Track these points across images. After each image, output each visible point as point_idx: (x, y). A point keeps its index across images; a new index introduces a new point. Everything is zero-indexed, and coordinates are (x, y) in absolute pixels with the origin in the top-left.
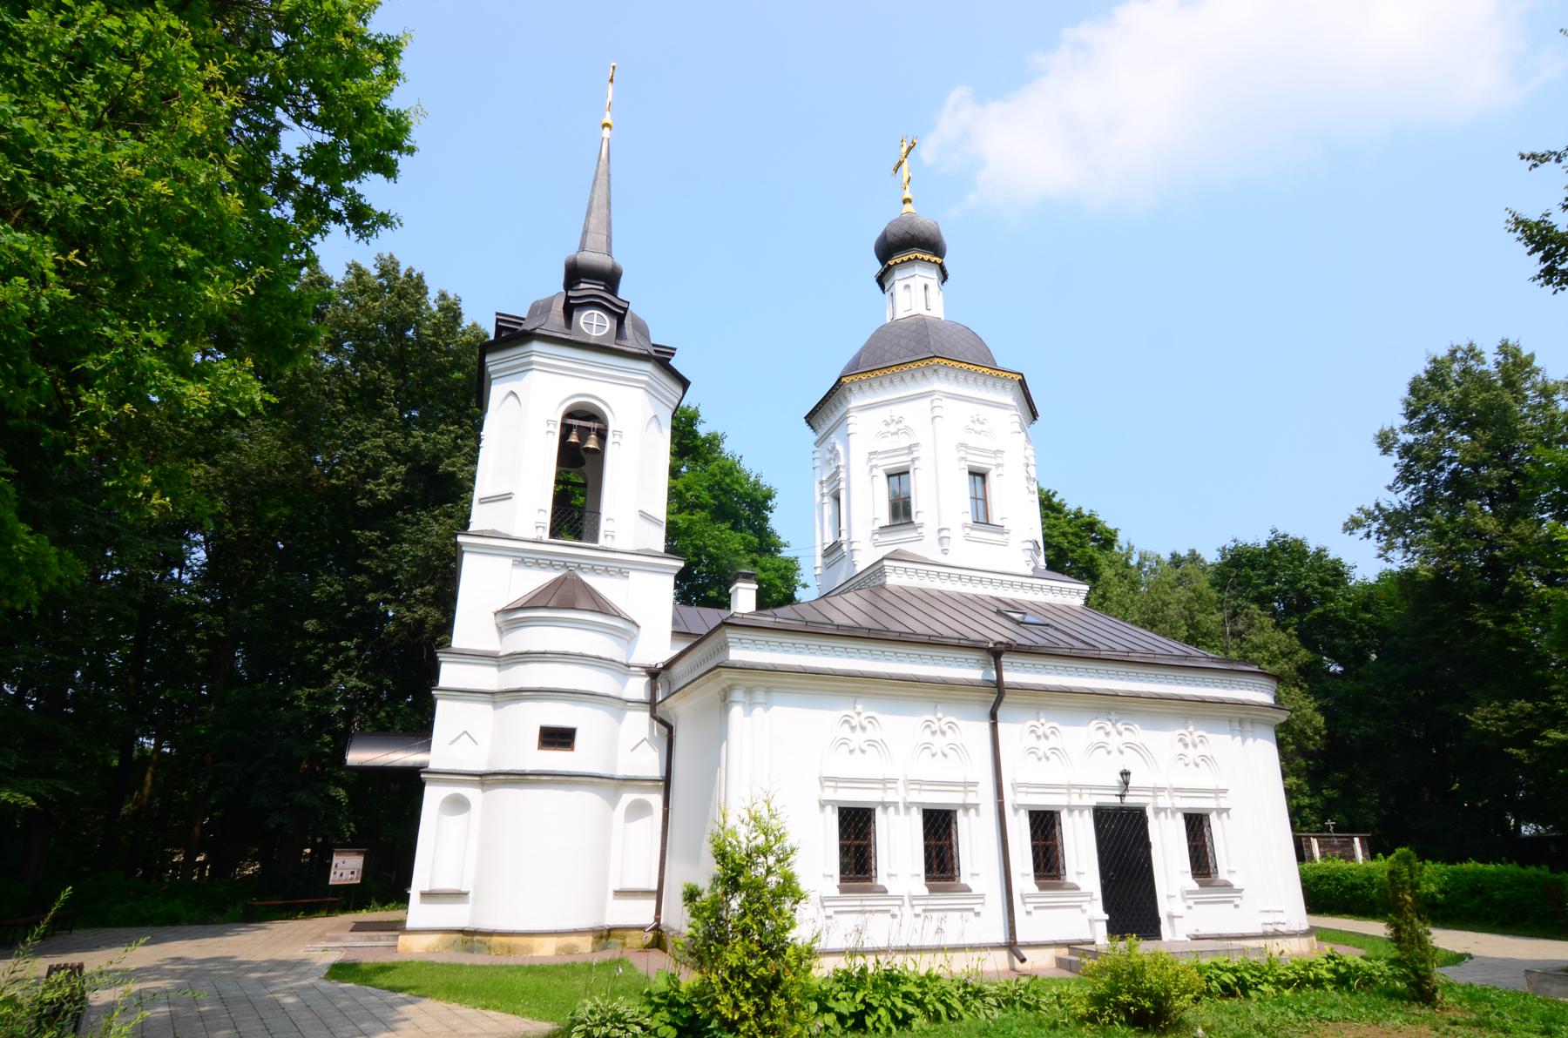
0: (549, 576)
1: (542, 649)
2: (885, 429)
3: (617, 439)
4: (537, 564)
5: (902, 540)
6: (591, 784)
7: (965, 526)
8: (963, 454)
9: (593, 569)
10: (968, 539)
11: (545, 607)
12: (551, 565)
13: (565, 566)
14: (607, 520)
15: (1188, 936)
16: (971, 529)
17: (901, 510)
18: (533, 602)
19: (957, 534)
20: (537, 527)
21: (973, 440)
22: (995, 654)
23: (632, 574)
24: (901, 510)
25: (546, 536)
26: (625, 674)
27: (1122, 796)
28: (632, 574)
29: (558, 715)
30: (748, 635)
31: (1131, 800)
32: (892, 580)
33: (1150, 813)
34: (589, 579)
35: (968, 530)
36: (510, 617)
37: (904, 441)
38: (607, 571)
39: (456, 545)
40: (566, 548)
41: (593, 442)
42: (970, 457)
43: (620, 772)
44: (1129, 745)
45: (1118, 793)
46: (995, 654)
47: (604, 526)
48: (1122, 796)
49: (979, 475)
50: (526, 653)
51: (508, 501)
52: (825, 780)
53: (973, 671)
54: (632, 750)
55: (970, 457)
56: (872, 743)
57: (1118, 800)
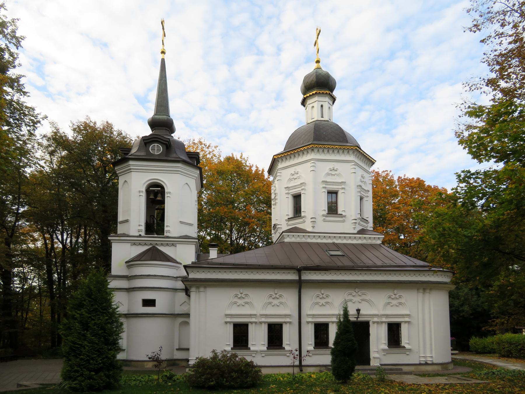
0: (146, 248)
1: (140, 274)
2: (292, 177)
3: (169, 195)
4: (140, 244)
5: (297, 223)
6: (170, 317)
7: (323, 215)
8: (324, 186)
9: (162, 245)
10: (324, 221)
11: (139, 260)
12: (145, 244)
13: (151, 244)
14: (167, 226)
15: (380, 364)
16: (326, 217)
17: (297, 210)
18: (140, 257)
19: (320, 219)
20: (139, 231)
21: (329, 179)
22: (299, 271)
23: (178, 245)
24: (297, 210)
25: (143, 234)
26: (176, 281)
27: (357, 318)
28: (178, 245)
29: (149, 295)
30: (194, 270)
31: (361, 319)
32: (287, 240)
33: (371, 323)
34: (161, 248)
35: (324, 218)
36: (130, 263)
37: (298, 182)
38: (167, 245)
39: (109, 240)
40: (154, 239)
41: (160, 197)
42: (328, 186)
43: (176, 313)
44: (363, 300)
45: (357, 317)
46: (299, 271)
47: (166, 229)
48: (357, 318)
49: (333, 193)
50: (141, 275)
51: (127, 223)
52: (227, 315)
53: (292, 276)
54: (180, 305)
55: (328, 186)
56: (247, 303)
57: (356, 319)
